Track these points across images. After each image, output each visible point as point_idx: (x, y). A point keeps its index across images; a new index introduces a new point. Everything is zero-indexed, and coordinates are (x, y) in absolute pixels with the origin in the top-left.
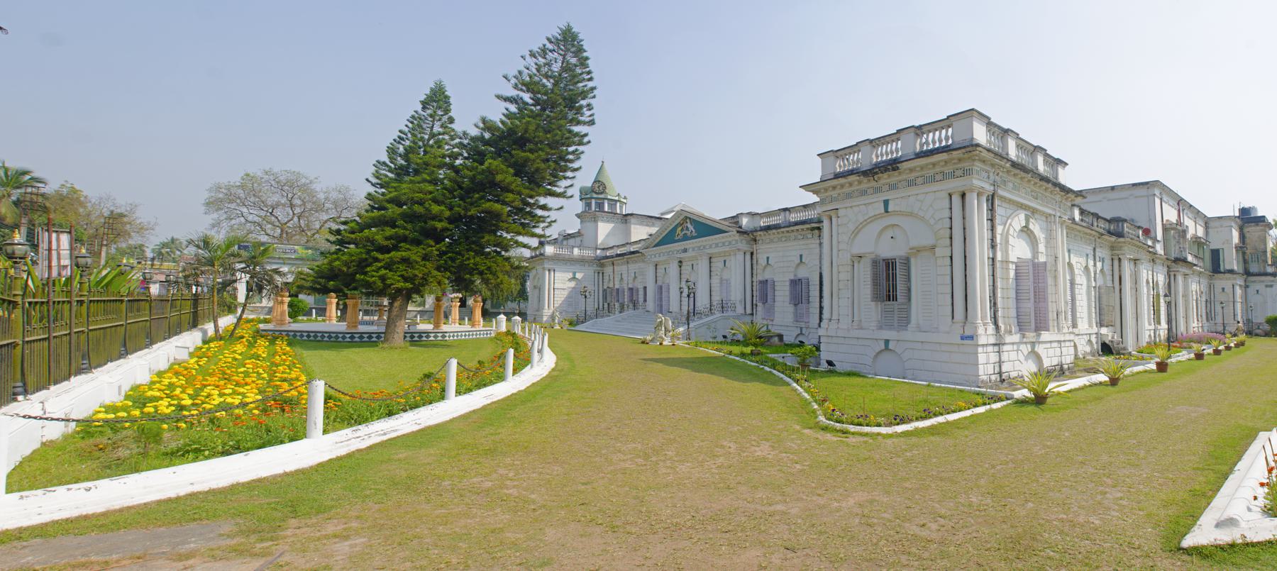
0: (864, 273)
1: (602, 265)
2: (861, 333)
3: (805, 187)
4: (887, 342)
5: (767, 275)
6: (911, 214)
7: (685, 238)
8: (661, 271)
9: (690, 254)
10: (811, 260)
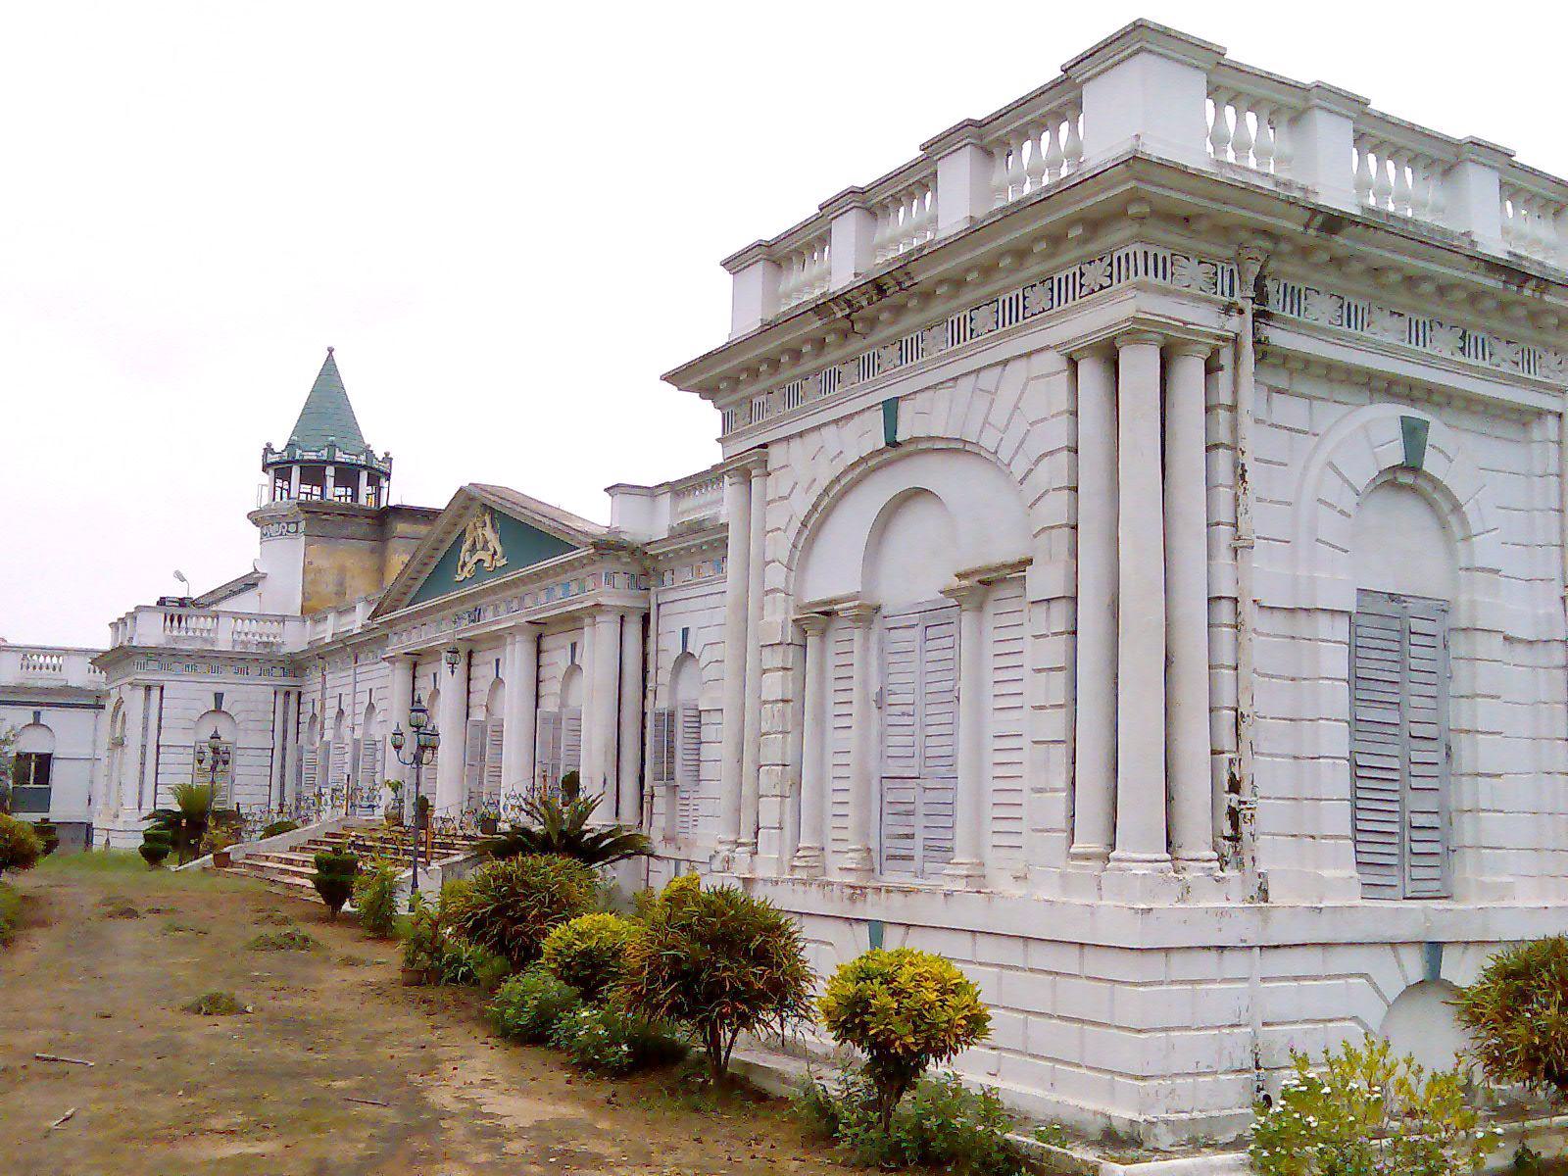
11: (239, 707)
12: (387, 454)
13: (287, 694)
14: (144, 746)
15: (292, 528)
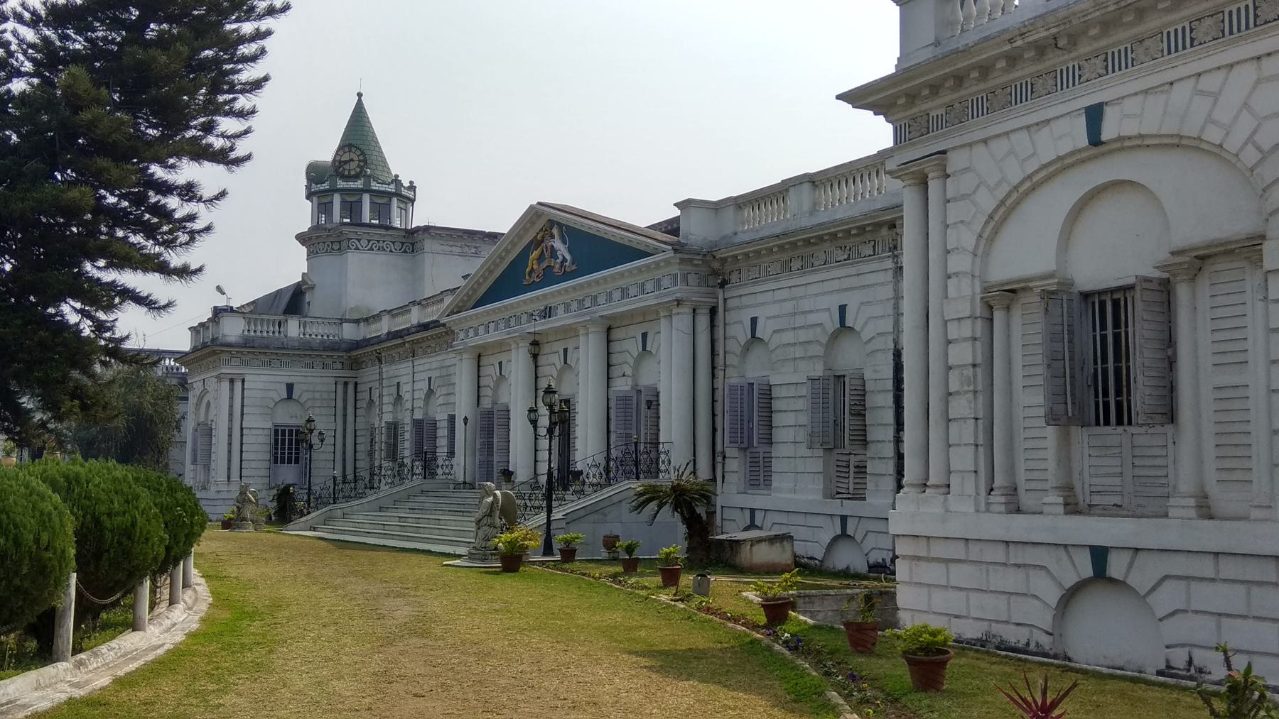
0: (1024, 333)
1: (355, 364)
2: (1019, 527)
3: (857, 98)
4: (1099, 555)
5: (755, 369)
6: (1176, 143)
7: (549, 278)
8: (490, 371)
9: (561, 319)
10: (870, 319)
11: (305, 397)
12: (411, 182)
13: (346, 384)
14: (230, 429)
15: (336, 247)
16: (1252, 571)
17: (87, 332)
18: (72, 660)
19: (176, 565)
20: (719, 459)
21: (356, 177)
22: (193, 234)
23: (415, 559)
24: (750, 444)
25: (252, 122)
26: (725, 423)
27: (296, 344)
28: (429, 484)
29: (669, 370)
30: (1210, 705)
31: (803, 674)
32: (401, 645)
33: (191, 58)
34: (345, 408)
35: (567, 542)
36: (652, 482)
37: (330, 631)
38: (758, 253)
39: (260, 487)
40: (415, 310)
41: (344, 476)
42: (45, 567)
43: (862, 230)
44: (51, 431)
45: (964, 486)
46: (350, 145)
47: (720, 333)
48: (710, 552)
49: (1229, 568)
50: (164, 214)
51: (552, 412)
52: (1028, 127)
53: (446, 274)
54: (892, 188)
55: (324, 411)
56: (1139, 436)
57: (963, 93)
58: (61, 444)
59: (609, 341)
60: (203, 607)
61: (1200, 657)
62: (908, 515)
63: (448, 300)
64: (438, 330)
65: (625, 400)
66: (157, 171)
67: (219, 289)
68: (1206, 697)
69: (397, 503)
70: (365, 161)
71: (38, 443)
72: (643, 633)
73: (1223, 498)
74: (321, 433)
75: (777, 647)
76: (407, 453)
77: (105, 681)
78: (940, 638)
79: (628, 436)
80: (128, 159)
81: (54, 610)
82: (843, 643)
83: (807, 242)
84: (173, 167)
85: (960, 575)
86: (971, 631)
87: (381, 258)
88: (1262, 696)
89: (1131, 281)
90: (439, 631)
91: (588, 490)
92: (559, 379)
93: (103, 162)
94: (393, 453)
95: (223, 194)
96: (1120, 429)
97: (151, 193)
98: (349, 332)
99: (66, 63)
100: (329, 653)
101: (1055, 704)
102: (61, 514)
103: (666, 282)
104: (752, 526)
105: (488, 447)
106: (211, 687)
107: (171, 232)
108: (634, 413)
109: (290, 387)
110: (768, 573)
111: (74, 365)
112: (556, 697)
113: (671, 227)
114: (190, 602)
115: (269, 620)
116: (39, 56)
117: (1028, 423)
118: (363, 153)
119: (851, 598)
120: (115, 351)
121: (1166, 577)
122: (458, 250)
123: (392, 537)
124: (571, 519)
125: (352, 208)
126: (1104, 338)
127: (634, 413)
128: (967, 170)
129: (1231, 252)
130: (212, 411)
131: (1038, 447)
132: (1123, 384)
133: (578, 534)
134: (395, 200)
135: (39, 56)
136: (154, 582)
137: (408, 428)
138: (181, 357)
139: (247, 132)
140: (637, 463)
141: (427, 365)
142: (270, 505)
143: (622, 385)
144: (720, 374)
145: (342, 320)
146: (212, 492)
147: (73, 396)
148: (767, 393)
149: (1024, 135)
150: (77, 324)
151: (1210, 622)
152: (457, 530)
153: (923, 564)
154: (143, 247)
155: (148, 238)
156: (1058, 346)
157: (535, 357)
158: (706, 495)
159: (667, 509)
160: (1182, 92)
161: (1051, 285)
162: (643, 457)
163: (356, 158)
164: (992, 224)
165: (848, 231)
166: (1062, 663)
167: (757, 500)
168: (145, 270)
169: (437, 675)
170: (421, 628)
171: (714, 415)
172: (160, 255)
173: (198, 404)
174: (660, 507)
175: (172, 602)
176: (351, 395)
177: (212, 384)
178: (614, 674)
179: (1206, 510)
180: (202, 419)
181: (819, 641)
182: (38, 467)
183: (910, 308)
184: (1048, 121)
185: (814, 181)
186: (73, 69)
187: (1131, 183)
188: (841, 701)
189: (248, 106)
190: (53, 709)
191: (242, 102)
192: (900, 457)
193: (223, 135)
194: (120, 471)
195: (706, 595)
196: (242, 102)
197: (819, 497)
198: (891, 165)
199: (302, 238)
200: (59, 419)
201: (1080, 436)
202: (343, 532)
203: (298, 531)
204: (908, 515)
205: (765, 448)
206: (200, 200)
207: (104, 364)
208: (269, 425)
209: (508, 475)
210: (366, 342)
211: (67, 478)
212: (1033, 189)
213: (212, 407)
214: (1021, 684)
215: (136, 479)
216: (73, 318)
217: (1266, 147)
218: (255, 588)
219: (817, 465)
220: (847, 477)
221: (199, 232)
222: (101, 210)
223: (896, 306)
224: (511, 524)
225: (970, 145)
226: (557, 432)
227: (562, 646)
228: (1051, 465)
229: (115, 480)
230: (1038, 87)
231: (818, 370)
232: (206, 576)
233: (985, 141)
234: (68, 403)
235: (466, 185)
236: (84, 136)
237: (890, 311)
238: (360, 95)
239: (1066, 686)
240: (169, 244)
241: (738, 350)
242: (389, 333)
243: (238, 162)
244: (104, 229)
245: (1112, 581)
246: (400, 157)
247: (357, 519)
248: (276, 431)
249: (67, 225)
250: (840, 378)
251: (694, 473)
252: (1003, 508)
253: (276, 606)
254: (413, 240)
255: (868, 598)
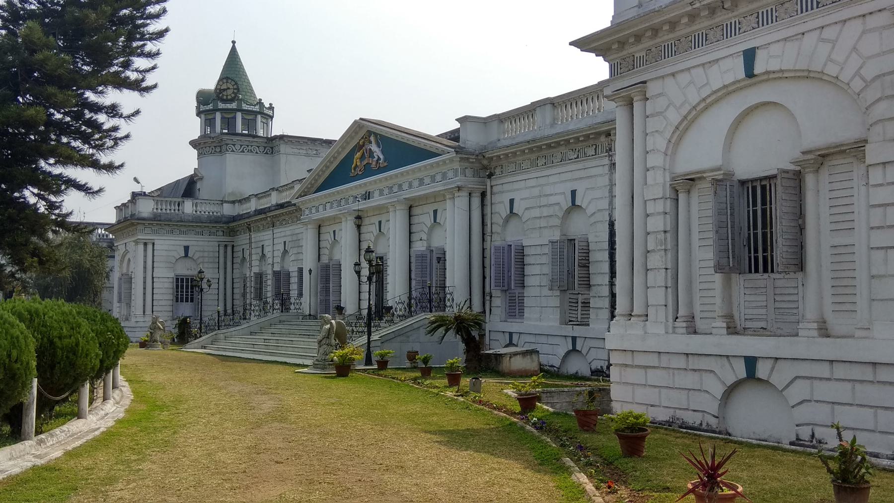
0: (700, 209)
1: (232, 232)
2: (695, 343)
3: (584, 44)
4: (751, 362)
5: (512, 235)
6: (807, 76)
7: (368, 171)
8: (327, 237)
9: (377, 200)
10: (592, 199)
12: (271, 104)
13: (226, 246)
14: (145, 278)
15: (218, 150)
16: (856, 373)
17: (42, 210)
18: (35, 439)
19: (107, 372)
20: (488, 298)
21: (231, 101)
22: (117, 141)
23: (276, 368)
24: (509, 288)
25: (157, 61)
26: (491, 273)
27: (190, 218)
28: (285, 316)
29: (452, 234)
30: (827, 465)
31: (546, 445)
32: (266, 429)
33: (113, 15)
34: (225, 263)
35: (382, 356)
36: (441, 314)
37: (216, 418)
38: (514, 153)
39: (166, 318)
40: (274, 194)
41: (225, 311)
42: (15, 375)
43: (587, 137)
44: (18, 280)
45: (658, 315)
46: (227, 78)
47: (488, 210)
48: (481, 362)
49: (840, 371)
50: (96, 126)
51: (371, 265)
52: (703, 65)
53: (296, 168)
54: (610, 108)
55: (211, 265)
56: (780, 280)
57: (658, 40)
58: (25, 289)
59: (410, 216)
60: (127, 402)
61: (820, 433)
62: (618, 337)
63: (297, 187)
64: (293, 208)
65: (422, 257)
66: (90, 96)
67: (136, 180)
68: (825, 460)
69: (262, 329)
70: (238, 89)
71: (9, 288)
72: (435, 419)
73: (836, 323)
74: (208, 281)
75: (528, 427)
76: (269, 294)
77: (58, 453)
78: (641, 420)
79: (424, 282)
80: (68, 87)
81: (22, 404)
82: (574, 424)
83: (549, 146)
84: (102, 92)
85: (654, 377)
86: (662, 415)
87: (250, 157)
88: (863, 459)
89: (774, 172)
90: (293, 417)
91: (396, 320)
92: (375, 243)
93: (51, 89)
94: (259, 295)
95: (137, 112)
96: (766, 275)
97: (86, 111)
98: (228, 210)
99: (25, 19)
100: (216, 433)
101: (720, 465)
102: (26, 338)
103: (450, 174)
104: (510, 344)
105: (326, 290)
106: (133, 457)
107: (100, 139)
108: (429, 266)
109: (186, 249)
110: (521, 376)
111: (33, 233)
112: (375, 463)
113: (454, 136)
114: (117, 398)
115: (174, 411)
116: (5, 14)
117: (703, 272)
118: (236, 84)
119: (579, 394)
120: (63, 223)
121: (796, 378)
122: (304, 152)
123: (259, 353)
124: (384, 340)
125: (229, 123)
126: (755, 212)
127: (429, 266)
128: (660, 95)
129: (844, 152)
130: (132, 265)
131: (709, 288)
132: (768, 244)
133: (390, 350)
134: (259, 117)
135: (5, 14)
136: (92, 384)
137: (270, 277)
138: (109, 227)
139: (154, 68)
140: (430, 301)
141: (283, 233)
142: (173, 331)
143: (419, 247)
144: (488, 238)
145: (223, 202)
146: (132, 323)
147: (33, 255)
148: (521, 252)
149: (701, 70)
150: (35, 204)
151: (827, 408)
152: (305, 348)
153: (628, 369)
154: (81, 150)
155: (84, 143)
156: (723, 218)
157: (359, 227)
158: (478, 323)
159: (451, 333)
160: (810, 40)
161: (719, 175)
162: (434, 297)
163: (231, 87)
164: (678, 132)
165: (577, 139)
166: (725, 436)
167: (514, 326)
168: (83, 166)
169: (292, 448)
170: (280, 415)
171: (484, 267)
172: (93, 155)
173: (122, 261)
174: (447, 331)
175: (105, 398)
176: (230, 255)
177: (131, 246)
178: (416, 447)
179: (824, 331)
180: (125, 271)
181: (557, 422)
182: (9, 305)
183: (620, 191)
184: (717, 60)
185: (552, 103)
186: (30, 23)
187: (775, 103)
188: (572, 464)
189: (154, 50)
190: (22, 473)
191: (150, 47)
192: (613, 296)
193: (137, 70)
194: (67, 307)
195: (479, 392)
196: (150, 47)
197: (557, 324)
198: (608, 91)
199: (194, 144)
200: (24, 270)
201: (740, 282)
202: (225, 349)
203: (193, 349)
204: (618, 337)
205: (519, 290)
206: (121, 116)
207: (55, 232)
208: (172, 275)
209: (340, 309)
210: (240, 217)
211: (30, 312)
212: (706, 108)
213: (132, 263)
214: (697, 452)
215: (79, 313)
216: (32, 200)
217: (869, 79)
218: (164, 388)
219: (556, 302)
220: (576, 310)
221: (121, 139)
222: (50, 123)
223: (611, 191)
224: (343, 343)
225: (663, 77)
226: (374, 279)
227: (379, 428)
228: (718, 301)
229: (63, 313)
230: (710, 36)
231: (556, 236)
232: (129, 381)
233: (673, 75)
234: (30, 260)
235: (309, 107)
236: (39, 71)
237: (607, 194)
238: (234, 42)
239: (728, 453)
240: (100, 148)
241: (501, 222)
242: (255, 211)
243: (148, 89)
244: (53, 137)
245: (759, 380)
246: (263, 85)
247: (235, 340)
248: (177, 279)
249: (27, 134)
250: (572, 241)
251: (470, 307)
252: (684, 330)
253: (178, 400)
254: (272, 145)
255: (591, 394)
